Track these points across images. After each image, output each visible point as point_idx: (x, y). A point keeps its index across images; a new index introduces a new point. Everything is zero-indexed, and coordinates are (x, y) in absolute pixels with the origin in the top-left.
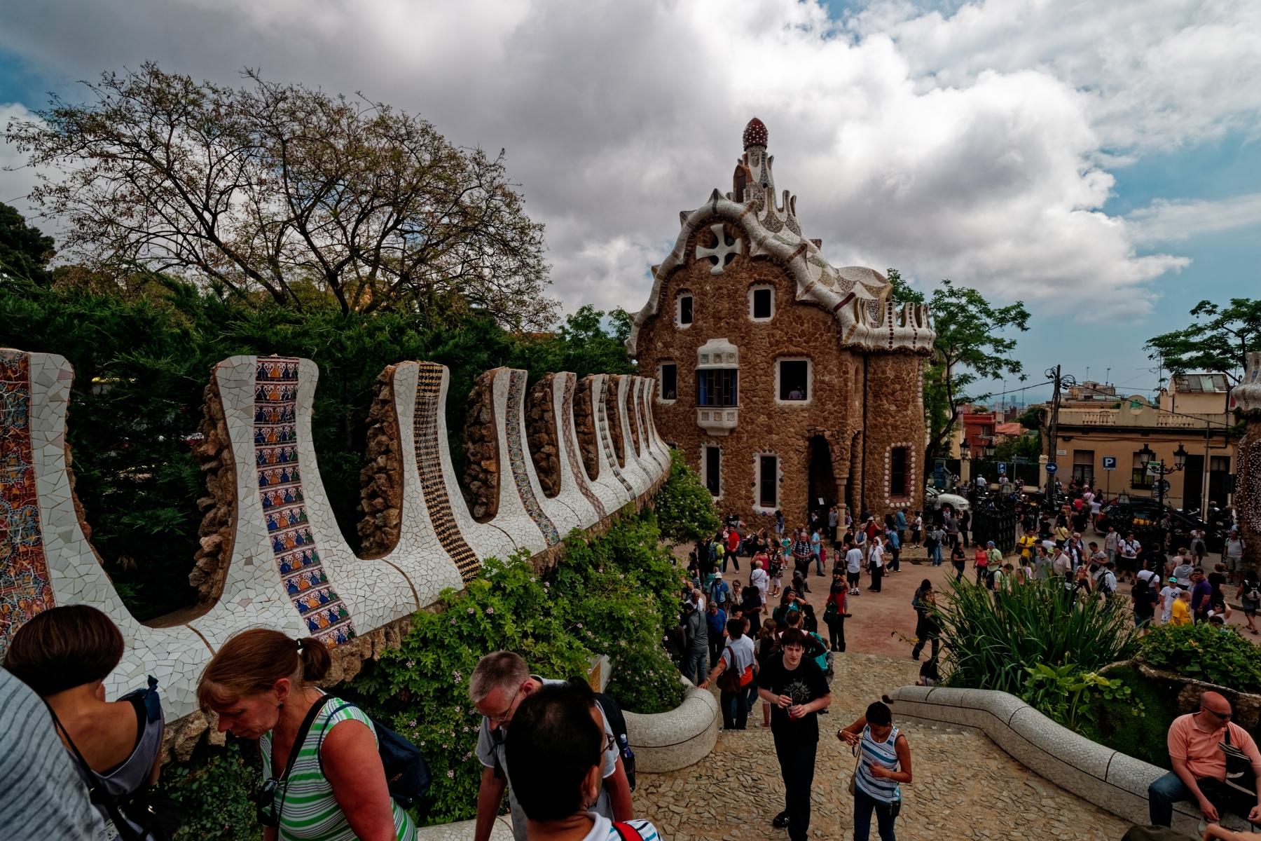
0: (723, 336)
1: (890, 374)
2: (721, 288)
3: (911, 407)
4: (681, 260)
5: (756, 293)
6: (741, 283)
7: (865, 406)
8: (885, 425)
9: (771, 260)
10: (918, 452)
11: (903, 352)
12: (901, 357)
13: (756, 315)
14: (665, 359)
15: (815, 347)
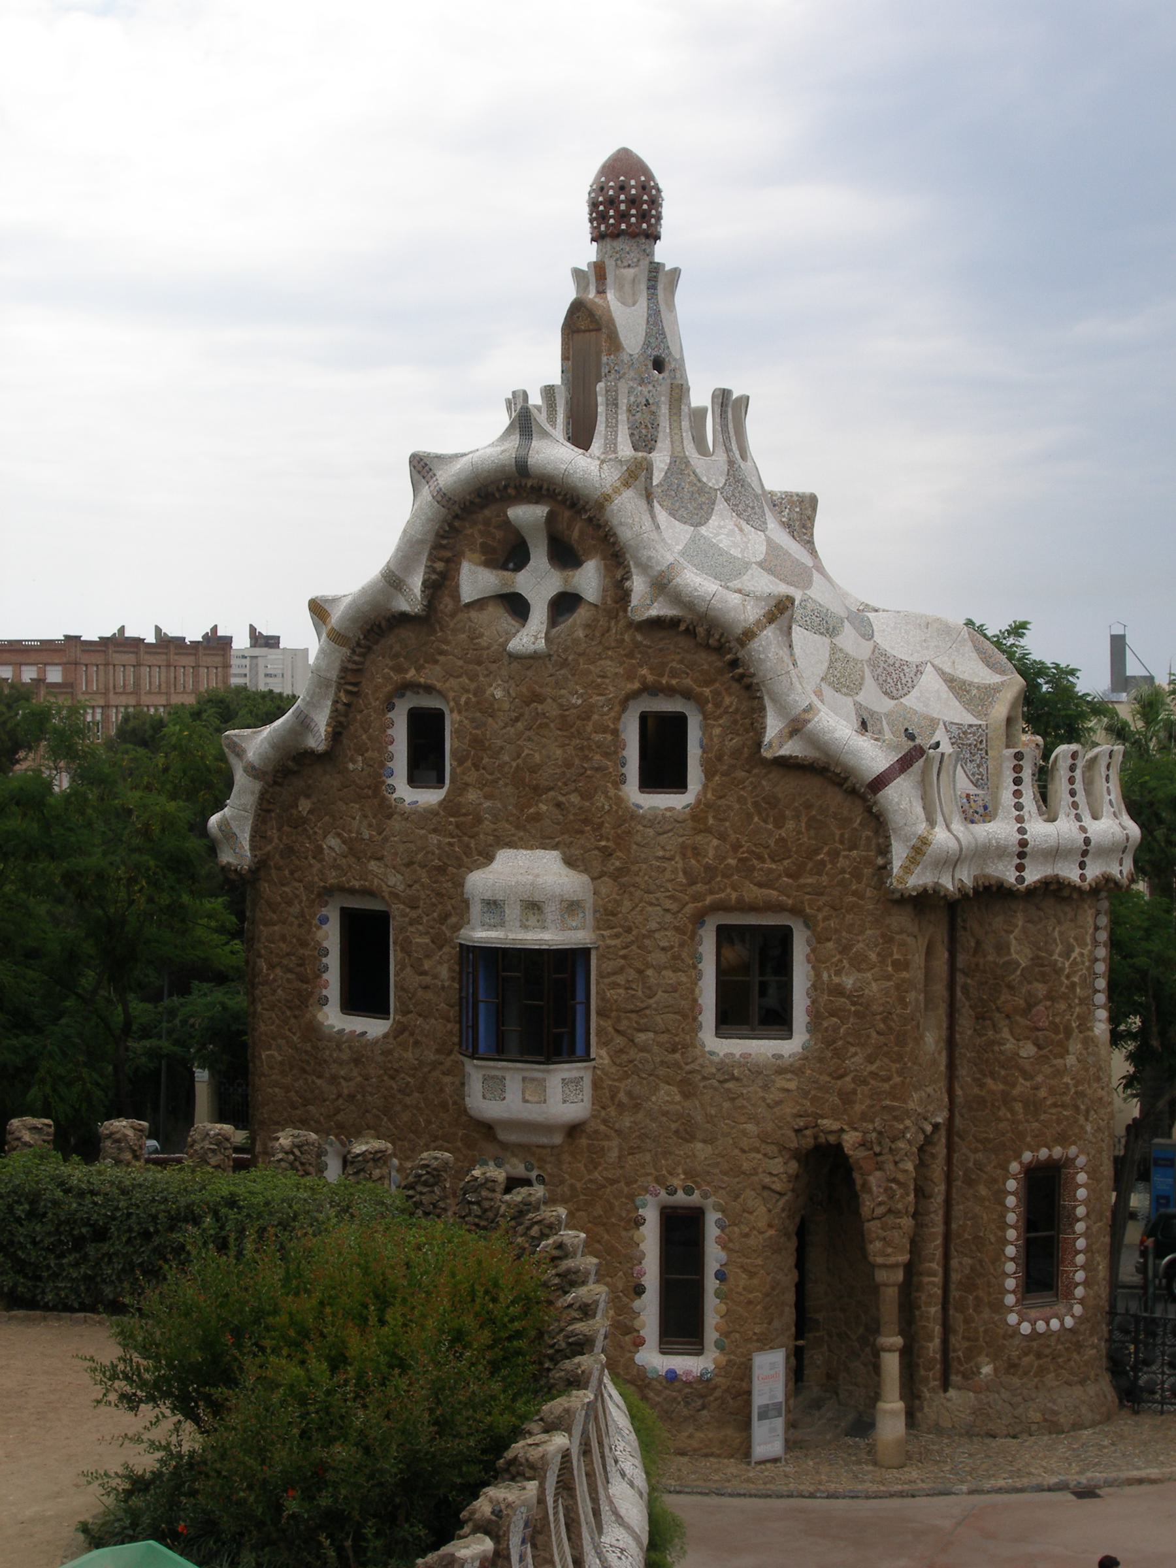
0: (545, 842)
1: (1020, 954)
2: (537, 698)
3: (1075, 1046)
4: (411, 600)
5: (644, 718)
6: (600, 690)
7: (951, 1044)
8: (1007, 1099)
10: (1093, 1174)
15: (819, 892)
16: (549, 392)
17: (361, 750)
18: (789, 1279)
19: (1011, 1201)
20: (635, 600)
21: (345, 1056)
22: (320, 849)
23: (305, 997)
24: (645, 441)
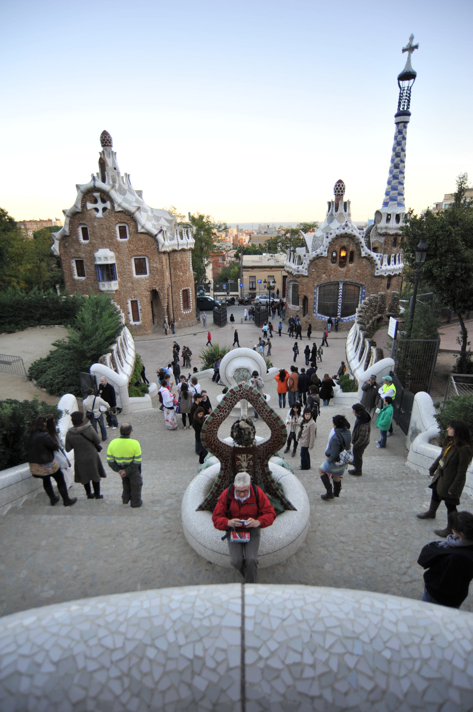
1: (179, 260)
2: (102, 225)
3: (188, 273)
5: (119, 227)
6: (112, 223)
7: (170, 274)
8: (179, 281)
9: (125, 213)
10: (192, 290)
11: (183, 250)
12: (183, 252)
13: (121, 238)
14: (77, 258)
15: (148, 252)
16: (97, 174)
17: (75, 235)
18: (150, 309)
19: (181, 295)
20: (116, 208)
21: (80, 283)
22: (70, 252)
23: (72, 275)
24: (114, 182)
